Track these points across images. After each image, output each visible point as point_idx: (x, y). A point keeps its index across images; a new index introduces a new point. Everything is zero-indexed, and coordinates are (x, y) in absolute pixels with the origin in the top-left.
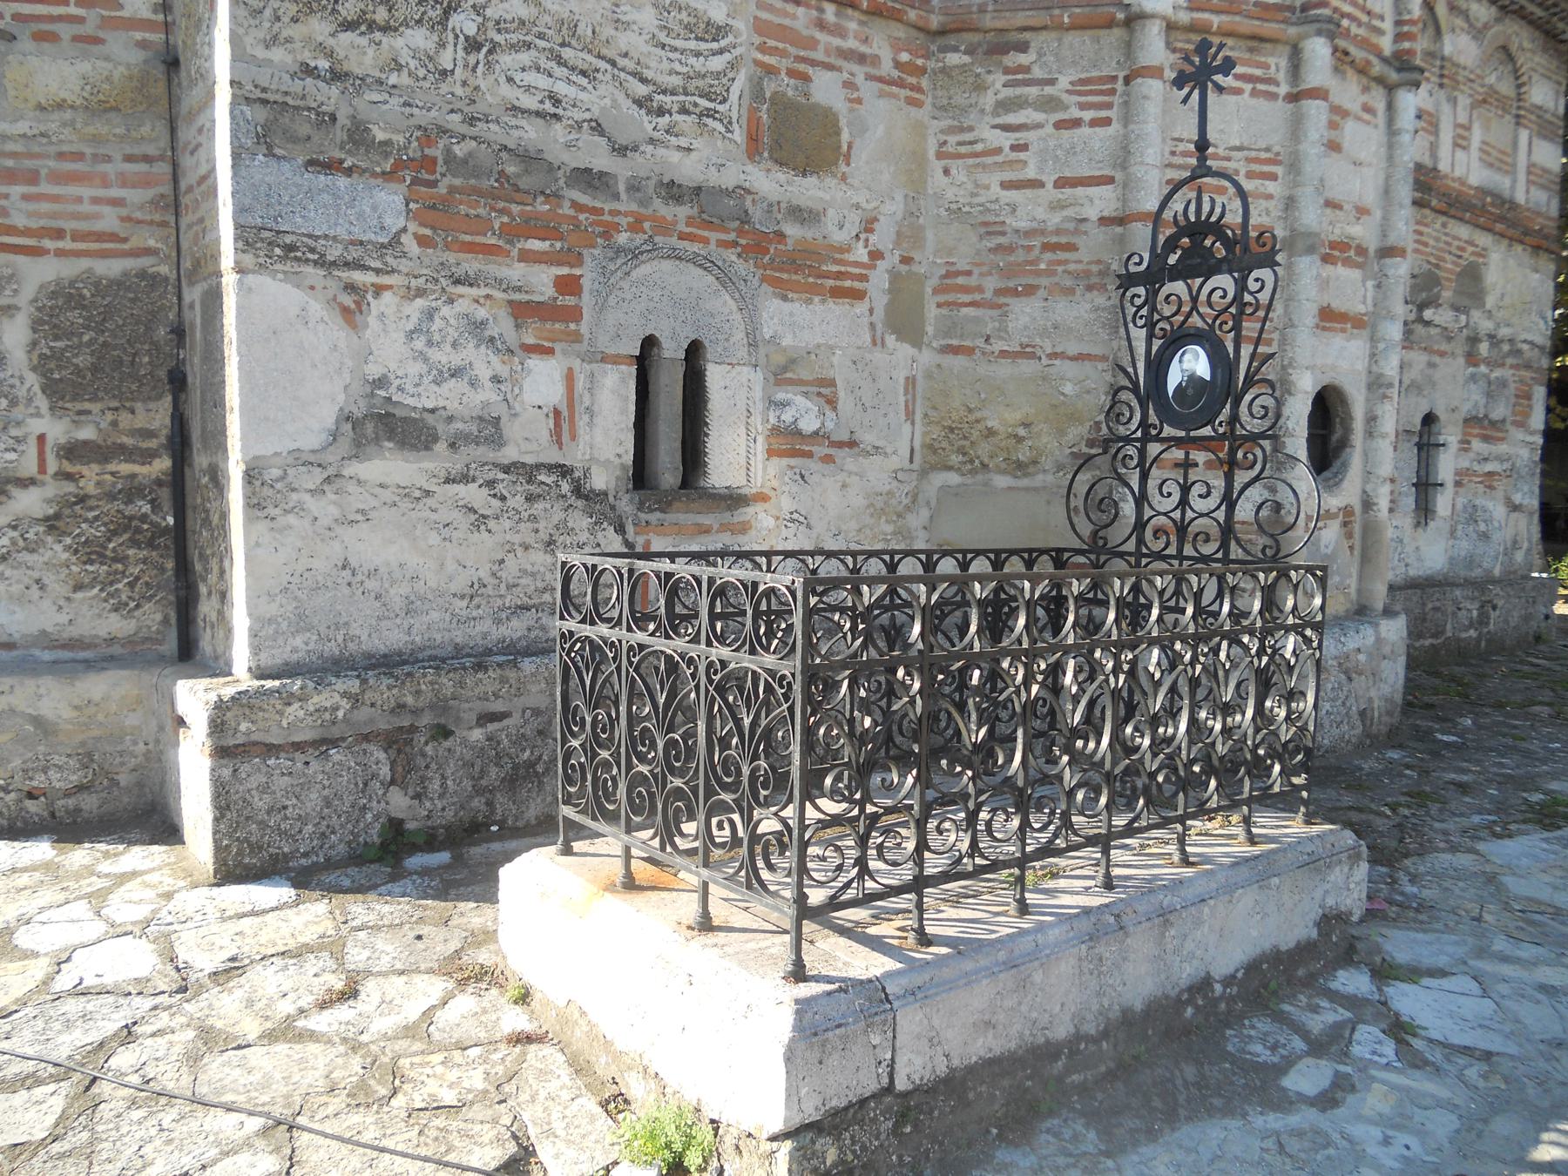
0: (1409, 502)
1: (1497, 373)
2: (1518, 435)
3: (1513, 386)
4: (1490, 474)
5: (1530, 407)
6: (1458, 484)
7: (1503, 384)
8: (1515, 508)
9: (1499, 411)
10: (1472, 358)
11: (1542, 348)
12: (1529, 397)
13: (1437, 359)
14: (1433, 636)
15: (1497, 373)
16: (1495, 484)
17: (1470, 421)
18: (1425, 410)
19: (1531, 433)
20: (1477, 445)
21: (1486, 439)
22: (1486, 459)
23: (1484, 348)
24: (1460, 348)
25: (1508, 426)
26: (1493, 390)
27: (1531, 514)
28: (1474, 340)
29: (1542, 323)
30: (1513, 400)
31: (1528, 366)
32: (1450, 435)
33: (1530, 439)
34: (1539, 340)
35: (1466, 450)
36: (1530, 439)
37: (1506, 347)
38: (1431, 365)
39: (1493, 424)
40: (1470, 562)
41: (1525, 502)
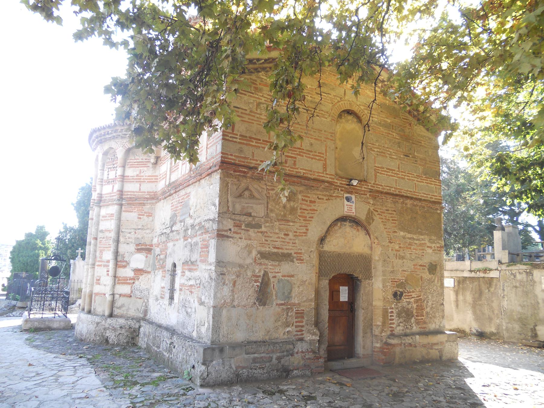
0: (167, 296)
1: (194, 240)
2: (203, 266)
3: (200, 243)
4: (191, 286)
5: (208, 252)
6: (181, 290)
7: (196, 244)
8: (202, 303)
9: (195, 257)
10: (185, 238)
11: (213, 220)
12: (207, 247)
13: (176, 243)
14: (157, 347)
15: (194, 240)
16: (193, 290)
17: (185, 263)
18: (172, 262)
19: (210, 264)
20: (187, 273)
21: (190, 270)
22: (190, 279)
23: (189, 232)
24: (182, 234)
25: (198, 263)
26: (192, 247)
27: (209, 308)
28: (186, 230)
29: (213, 207)
30: (200, 250)
31: (207, 232)
32: (179, 271)
33: (209, 267)
34: (212, 217)
35: (183, 276)
36: (209, 267)
37: (197, 228)
38: (174, 245)
39: (192, 263)
40: (183, 325)
41: (207, 301)
